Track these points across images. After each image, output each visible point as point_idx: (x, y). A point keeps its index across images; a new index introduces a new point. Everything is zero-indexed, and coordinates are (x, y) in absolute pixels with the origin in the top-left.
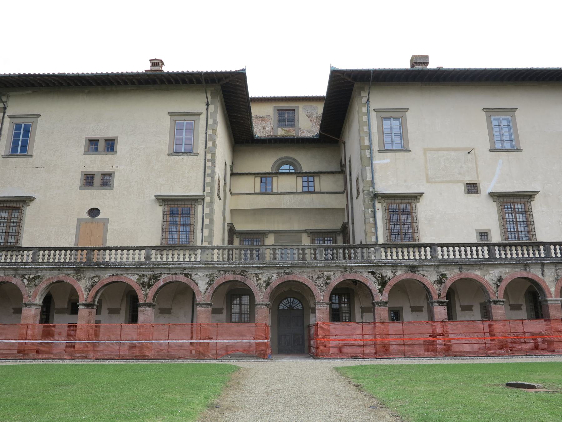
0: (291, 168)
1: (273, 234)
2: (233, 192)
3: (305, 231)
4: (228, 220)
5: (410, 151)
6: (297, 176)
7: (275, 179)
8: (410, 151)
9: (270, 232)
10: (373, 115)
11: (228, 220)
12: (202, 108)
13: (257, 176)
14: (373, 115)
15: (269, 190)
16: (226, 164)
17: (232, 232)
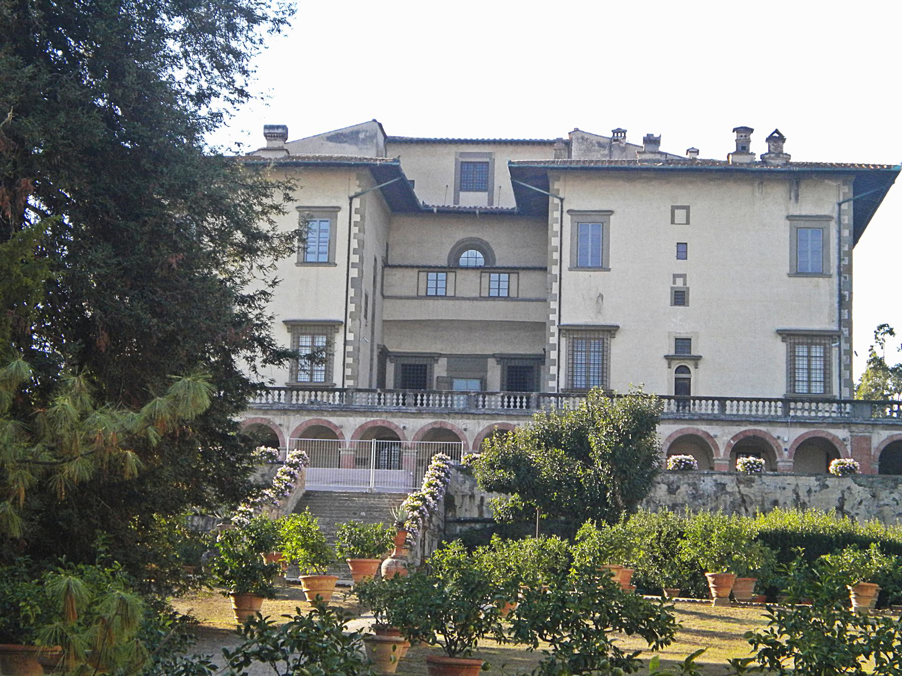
0: (479, 254)
1: (446, 359)
2: (386, 294)
3: (494, 356)
4: (377, 341)
5: (609, 270)
6: (482, 272)
7: (451, 276)
8: (609, 270)
9: (441, 355)
12: (345, 205)
13: (422, 270)
14: (567, 218)
16: (375, 260)
17: (384, 354)
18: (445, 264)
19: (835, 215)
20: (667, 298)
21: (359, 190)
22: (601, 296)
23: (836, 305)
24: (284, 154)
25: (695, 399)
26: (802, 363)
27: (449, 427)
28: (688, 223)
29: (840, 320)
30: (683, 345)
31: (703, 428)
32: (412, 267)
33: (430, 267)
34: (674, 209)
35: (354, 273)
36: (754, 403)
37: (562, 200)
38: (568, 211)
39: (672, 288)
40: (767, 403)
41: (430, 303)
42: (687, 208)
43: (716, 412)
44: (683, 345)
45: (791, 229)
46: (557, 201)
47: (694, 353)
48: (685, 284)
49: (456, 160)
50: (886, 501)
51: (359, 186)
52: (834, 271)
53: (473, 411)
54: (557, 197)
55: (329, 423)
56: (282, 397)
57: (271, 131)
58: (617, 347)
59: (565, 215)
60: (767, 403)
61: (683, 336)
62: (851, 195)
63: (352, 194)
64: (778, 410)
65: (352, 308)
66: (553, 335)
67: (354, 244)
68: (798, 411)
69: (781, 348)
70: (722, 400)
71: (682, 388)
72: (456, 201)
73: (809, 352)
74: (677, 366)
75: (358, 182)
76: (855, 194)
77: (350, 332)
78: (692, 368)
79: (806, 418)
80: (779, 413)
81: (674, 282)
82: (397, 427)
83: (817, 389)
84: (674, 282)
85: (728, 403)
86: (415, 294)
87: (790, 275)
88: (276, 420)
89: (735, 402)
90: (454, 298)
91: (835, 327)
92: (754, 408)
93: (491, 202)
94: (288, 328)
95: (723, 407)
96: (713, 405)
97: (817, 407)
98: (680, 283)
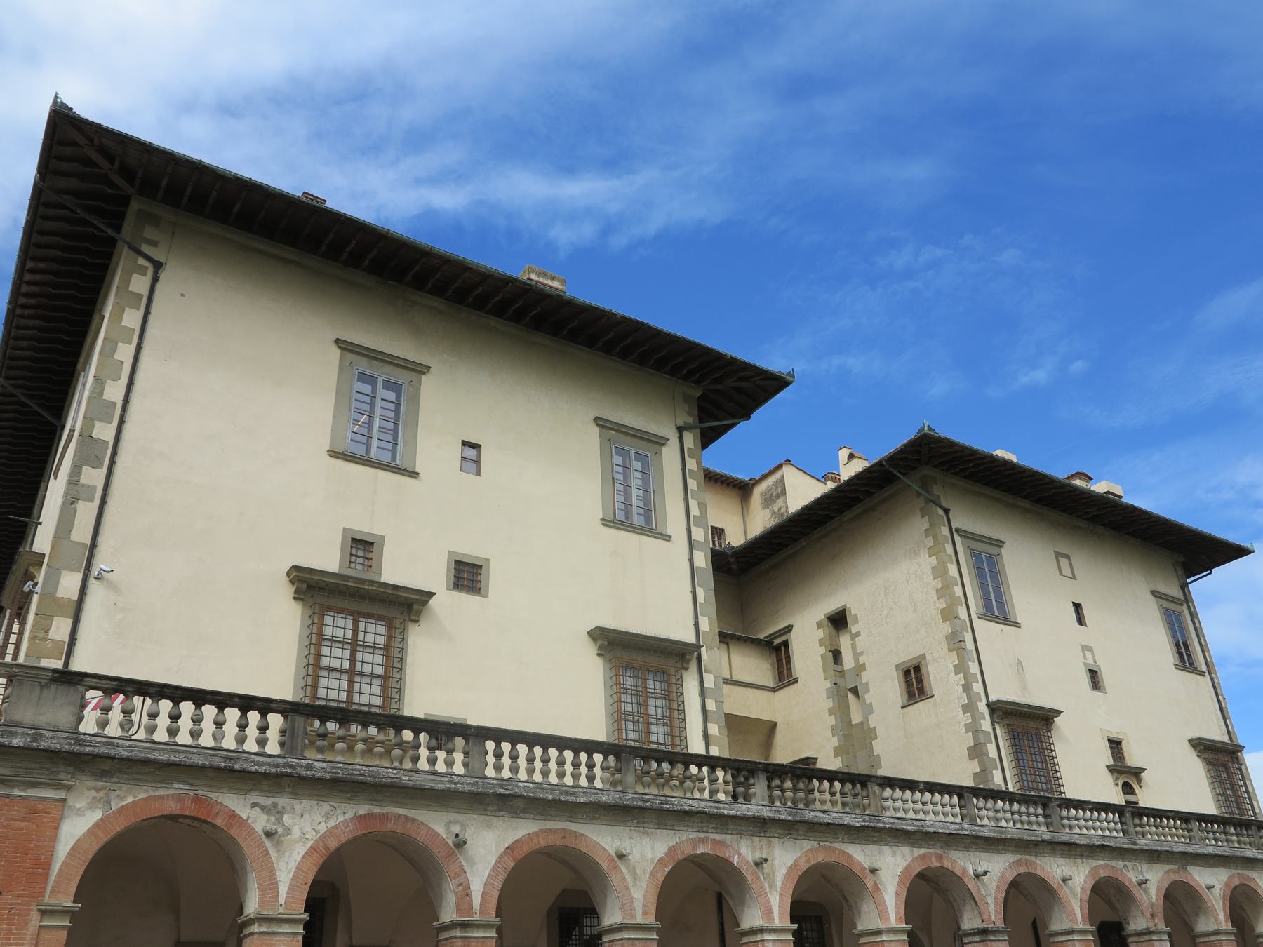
5: (1016, 625)
8: (1016, 625)
10: (957, 538)
14: (957, 538)
21: (690, 420)
22: (1020, 663)
23: (1219, 712)
27: (1040, 873)
28: (1074, 578)
37: (947, 511)
46: (941, 512)
48: (1095, 662)
51: (689, 414)
52: (1204, 668)
54: (941, 507)
55: (849, 857)
57: (541, 279)
63: (680, 423)
65: (704, 624)
74: (1122, 782)
77: (708, 672)
78: (1136, 787)
82: (965, 871)
94: (600, 648)
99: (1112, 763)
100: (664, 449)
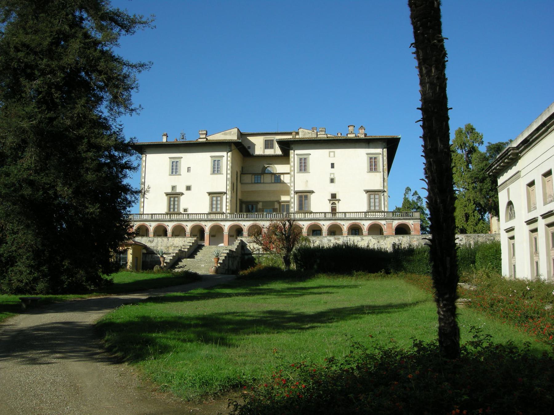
4: (239, 197)
7: (262, 176)
9: (260, 202)
10: (296, 156)
11: (239, 197)
14: (296, 156)
15: (259, 181)
16: (237, 172)
18: (260, 172)
19: (381, 153)
20: (329, 181)
24: (205, 140)
25: (338, 213)
26: (372, 200)
28: (334, 156)
29: (384, 186)
30: (334, 196)
31: (339, 222)
32: (250, 174)
33: (255, 174)
34: (330, 152)
35: (229, 176)
36: (355, 214)
38: (297, 154)
39: (330, 178)
40: (359, 213)
41: (256, 185)
42: (334, 152)
43: (343, 217)
44: (334, 196)
45: (367, 157)
47: (337, 198)
49: (264, 139)
50: (382, 244)
52: (381, 170)
53: (265, 219)
55: (220, 224)
56: (205, 216)
58: (312, 197)
59: (295, 156)
60: (359, 213)
61: (334, 193)
62: (386, 146)
64: (363, 216)
65: (228, 187)
66: (292, 194)
67: (229, 167)
68: (370, 216)
69: (365, 196)
70: (345, 213)
71: (334, 210)
72: (264, 152)
73: (375, 196)
75: (229, 148)
76: (387, 146)
79: (372, 218)
80: (363, 216)
81: (331, 176)
82: (241, 225)
83: (377, 208)
84: (331, 176)
85: (347, 214)
86: (250, 182)
87: (367, 172)
88: (147, 224)
89: (349, 214)
90: (263, 183)
91: (382, 188)
92: (355, 215)
93: (275, 151)
95: (345, 215)
96: (342, 215)
97: (375, 214)
98: (332, 177)
99: (330, 198)
100: (223, 158)
